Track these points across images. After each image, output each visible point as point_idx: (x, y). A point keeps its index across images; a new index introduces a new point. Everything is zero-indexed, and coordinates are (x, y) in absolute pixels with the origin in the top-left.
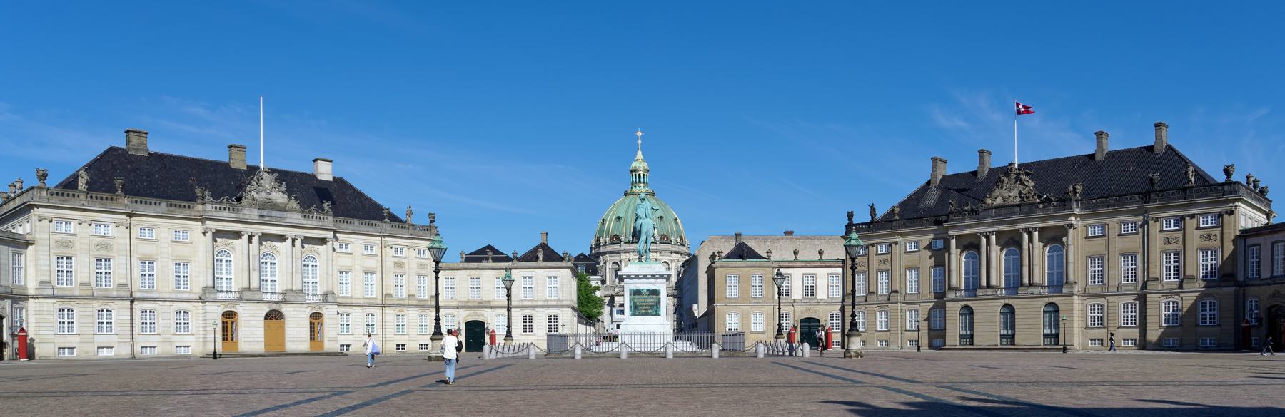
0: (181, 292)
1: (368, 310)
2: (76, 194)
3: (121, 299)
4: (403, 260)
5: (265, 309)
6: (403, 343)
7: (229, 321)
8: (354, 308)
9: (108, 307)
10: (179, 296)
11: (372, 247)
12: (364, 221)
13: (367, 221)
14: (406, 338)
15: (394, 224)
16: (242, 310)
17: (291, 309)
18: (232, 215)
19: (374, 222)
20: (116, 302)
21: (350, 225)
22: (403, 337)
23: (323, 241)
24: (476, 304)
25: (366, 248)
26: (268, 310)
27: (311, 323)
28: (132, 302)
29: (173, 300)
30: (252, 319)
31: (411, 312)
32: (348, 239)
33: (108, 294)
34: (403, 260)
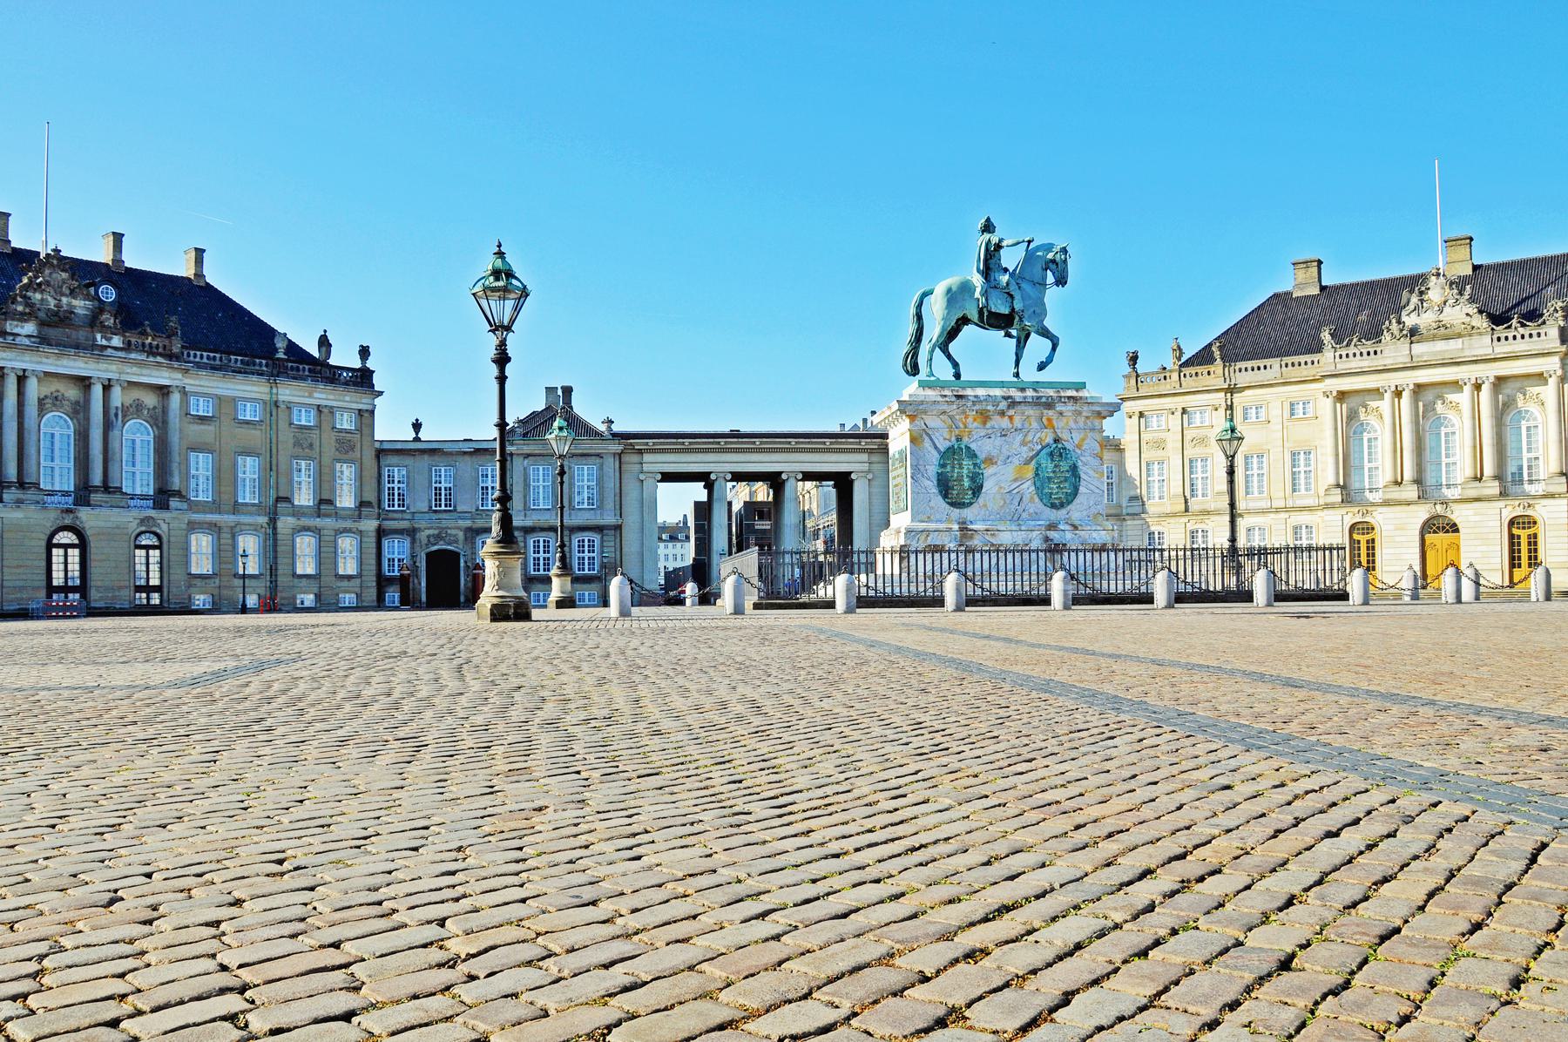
0: (1301, 497)
2: (1167, 375)
3: (1218, 513)
5: (1422, 513)
7: (1363, 539)
9: (1202, 526)
10: (1299, 503)
16: (1381, 519)
17: (1471, 512)
18: (1366, 363)
20: (1213, 518)
23: (1540, 378)
26: (1427, 516)
27: (1511, 536)
29: (1286, 509)
30: (1398, 532)
33: (1207, 507)
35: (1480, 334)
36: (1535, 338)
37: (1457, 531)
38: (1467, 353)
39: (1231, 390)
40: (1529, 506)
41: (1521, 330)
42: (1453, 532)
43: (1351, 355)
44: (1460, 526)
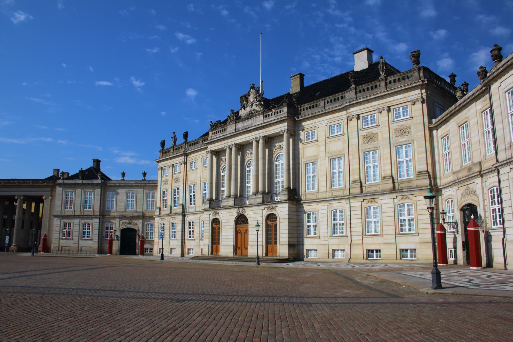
1: (334, 205)
4: (375, 130)
6: (377, 247)
8: (320, 204)
11: (339, 125)
12: (328, 99)
13: (332, 97)
14: (380, 240)
15: (360, 88)
19: (339, 95)
21: (315, 108)
22: (376, 240)
24: (465, 173)
25: (331, 128)
28: (184, 216)
31: (383, 202)
32: (312, 125)
34: (375, 130)
35: (259, 115)
36: (279, 114)
37: (248, 223)
38: (254, 125)
39: (186, 155)
40: (273, 208)
41: (273, 110)
42: (245, 224)
43: (217, 132)
44: (249, 220)
